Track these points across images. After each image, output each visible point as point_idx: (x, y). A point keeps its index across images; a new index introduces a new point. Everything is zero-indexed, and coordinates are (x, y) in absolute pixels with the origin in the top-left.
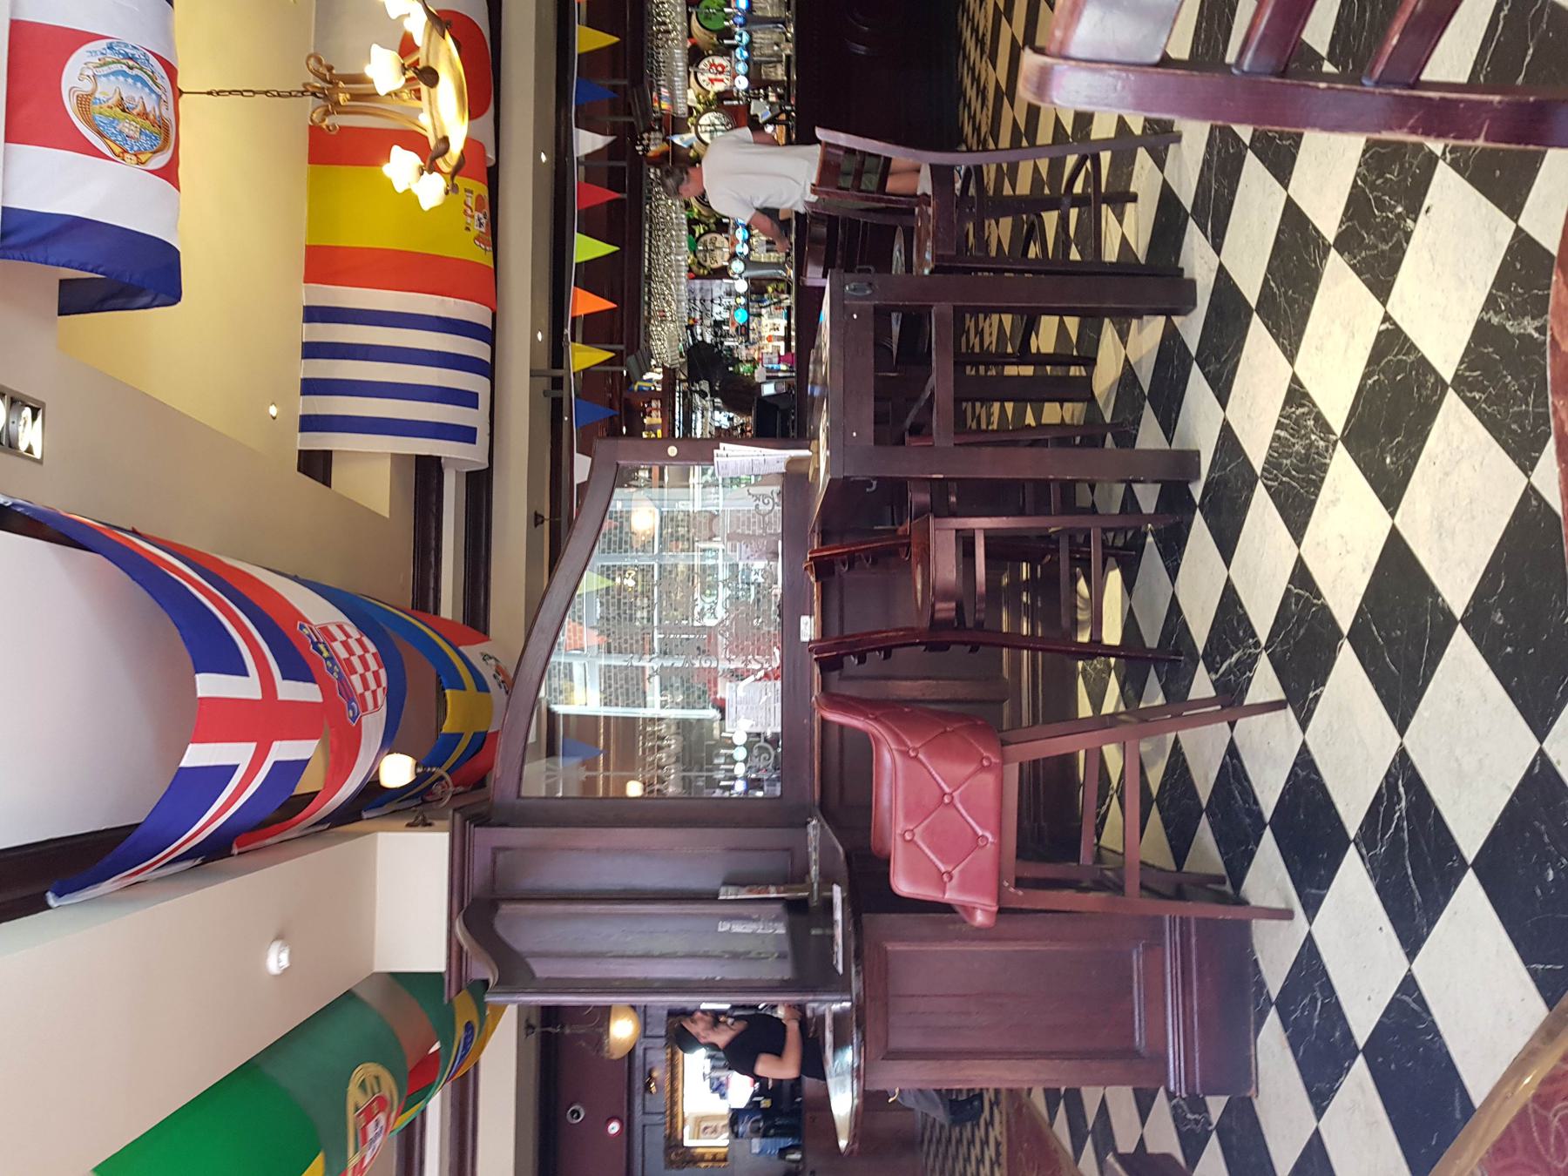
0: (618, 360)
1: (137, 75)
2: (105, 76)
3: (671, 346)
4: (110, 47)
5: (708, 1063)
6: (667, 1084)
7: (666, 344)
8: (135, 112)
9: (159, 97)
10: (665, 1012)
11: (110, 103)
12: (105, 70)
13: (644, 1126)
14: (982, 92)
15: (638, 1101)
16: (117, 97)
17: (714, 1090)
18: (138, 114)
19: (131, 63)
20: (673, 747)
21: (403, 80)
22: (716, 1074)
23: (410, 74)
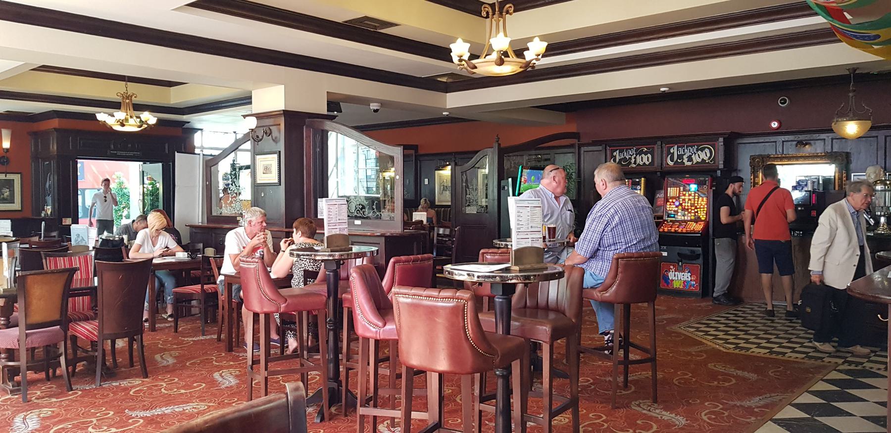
6: (801, 154)
10: (849, 151)
13: (776, 142)
15: (791, 137)
17: (798, 183)
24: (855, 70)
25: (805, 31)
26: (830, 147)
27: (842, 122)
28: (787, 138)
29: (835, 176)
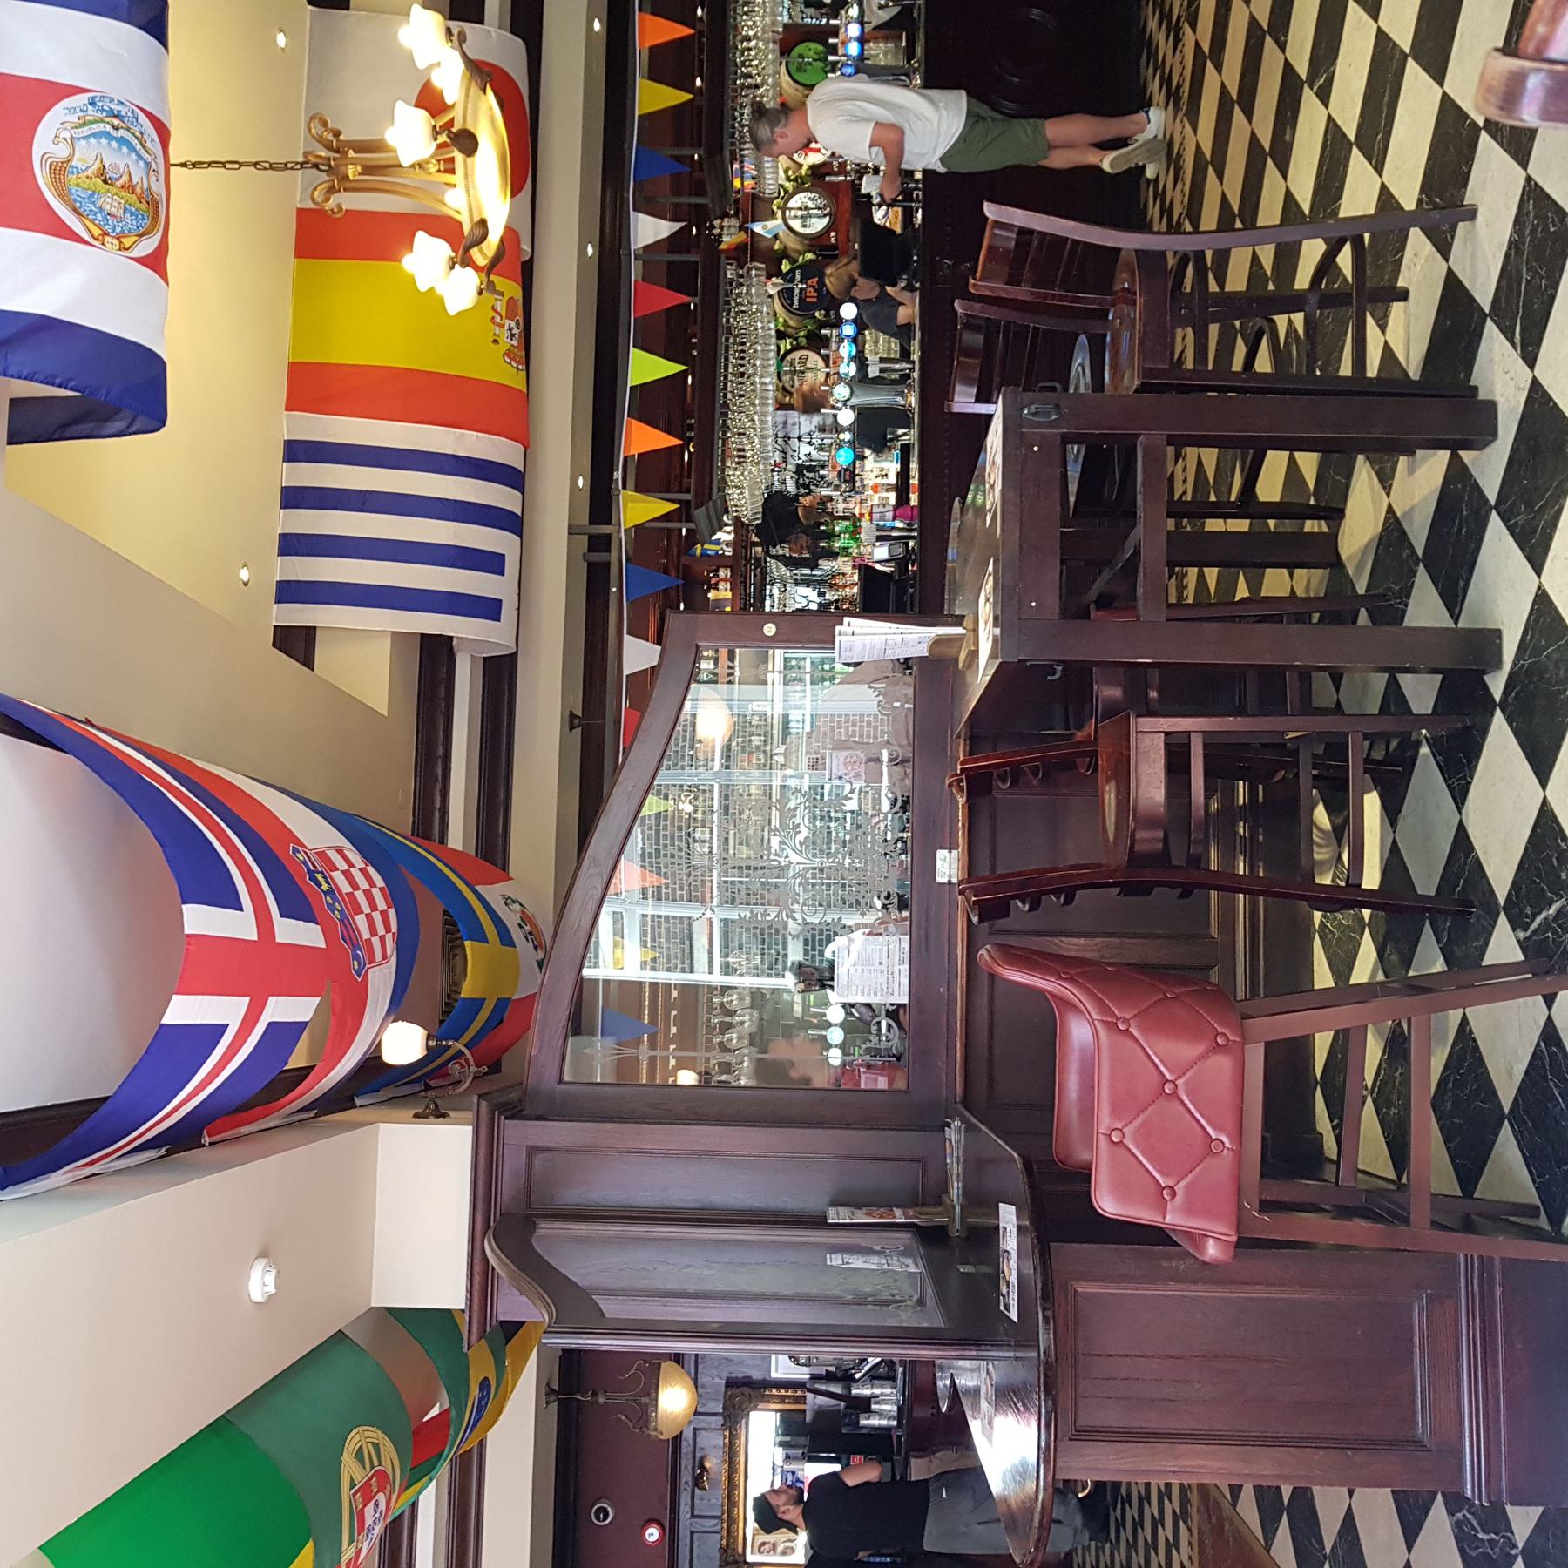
0: (684, 513)
3: (752, 495)
5: (779, 1453)
7: (747, 493)
10: (724, 1382)
13: (692, 1533)
15: (685, 1499)
20: (746, 1024)
21: (434, 144)
22: (793, 1467)
23: (443, 138)
24: (552, 1390)
25: (450, 1493)
26: (714, 1418)
27: (659, 1421)
28: (684, 1508)
29: (777, 1411)
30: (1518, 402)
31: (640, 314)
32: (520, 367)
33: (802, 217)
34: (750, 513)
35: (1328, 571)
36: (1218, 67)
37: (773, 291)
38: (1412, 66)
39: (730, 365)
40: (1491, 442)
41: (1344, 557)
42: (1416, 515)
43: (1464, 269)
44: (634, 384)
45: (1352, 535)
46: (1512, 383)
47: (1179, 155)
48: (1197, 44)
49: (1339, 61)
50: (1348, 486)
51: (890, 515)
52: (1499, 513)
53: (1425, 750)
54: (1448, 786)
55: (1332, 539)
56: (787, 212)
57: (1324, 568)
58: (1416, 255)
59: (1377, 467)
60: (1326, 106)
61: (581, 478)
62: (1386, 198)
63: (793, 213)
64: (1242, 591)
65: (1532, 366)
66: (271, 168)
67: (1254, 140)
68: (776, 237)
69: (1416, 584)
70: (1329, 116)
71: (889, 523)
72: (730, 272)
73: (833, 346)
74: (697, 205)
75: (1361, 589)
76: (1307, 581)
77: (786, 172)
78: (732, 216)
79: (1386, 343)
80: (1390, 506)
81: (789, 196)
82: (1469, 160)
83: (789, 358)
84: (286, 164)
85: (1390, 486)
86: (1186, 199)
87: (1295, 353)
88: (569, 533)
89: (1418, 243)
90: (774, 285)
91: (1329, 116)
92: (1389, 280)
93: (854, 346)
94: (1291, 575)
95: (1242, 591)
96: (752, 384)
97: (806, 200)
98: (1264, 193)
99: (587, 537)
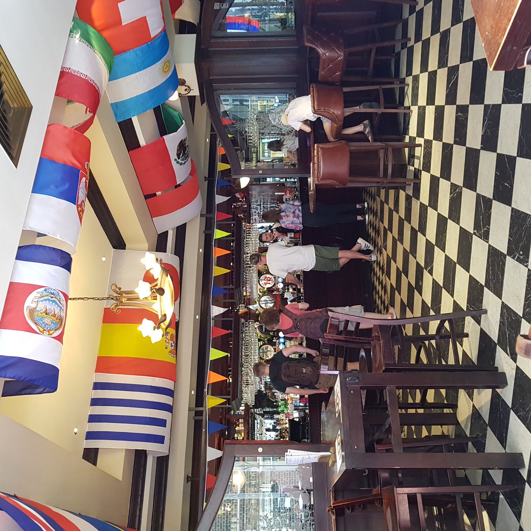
0: (228, 402)
1: (54, 300)
2: (41, 301)
3: (251, 396)
4: (45, 290)
7: (249, 395)
8: (51, 314)
9: (61, 308)
11: (41, 312)
12: (42, 299)
14: (384, 288)
16: (45, 309)
18: (52, 315)
19: (52, 296)
30: (513, 373)
31: (213, 337)
32: (174, 356)
33: (265, 303)
34: (251, 402)
35: (455, 426)
36: (395, 262)
37: (256, 326)
38: (458, 267)
39: (243, 353)
40: (506, 386)
41: (460, 421)
42: (484, 409)
43: (486, 329)
44: (211, 359)
45: (461, 414)
46: (510, 367)
47: (385, 286)
48: (387, 255)
49: (434, 263)
50: (457, 397)
51: (298, 401)
52: (513, 411)
53: (501, 496)
54: (513, 511)
55: (454, 415)
56: (260, 302)
57: (453, 425)
58: (469, 323)
59: (467, 391)
60: (432, 276)
61: (193, 391)
62: (456, 305)
63: (262, 302)
64: (425, 433)
65: (515, 362)
66: (98, 299)
67: (409, 284)
68: (257, 310)
69: (487, 434)
70: (433, 279)
71: (298, 404)
72: (243, 320)
73: (277, 345)
74: (231, 302)
75: (468, 433)
76: (448, 430)
77: (260, 290)
78: (243, 303)
79: (463, 350)
80: (473, 405)
81: (260, 297)
82: (482, 295)
83: (262, 347)
84: (103, 298)
85: (473, 398)
86: (389, 300)
87: (432, 351)
88: (189, 410)
89: (469, 320)
90: (256, 324)
91: (433, 279)
92: (461, 330)
93: (284, 345)
94: (442, 427)
95: (425, 433)
96: (251, 359)
97: (266, 298)
98: (415, 300)
99: (194, 411)
